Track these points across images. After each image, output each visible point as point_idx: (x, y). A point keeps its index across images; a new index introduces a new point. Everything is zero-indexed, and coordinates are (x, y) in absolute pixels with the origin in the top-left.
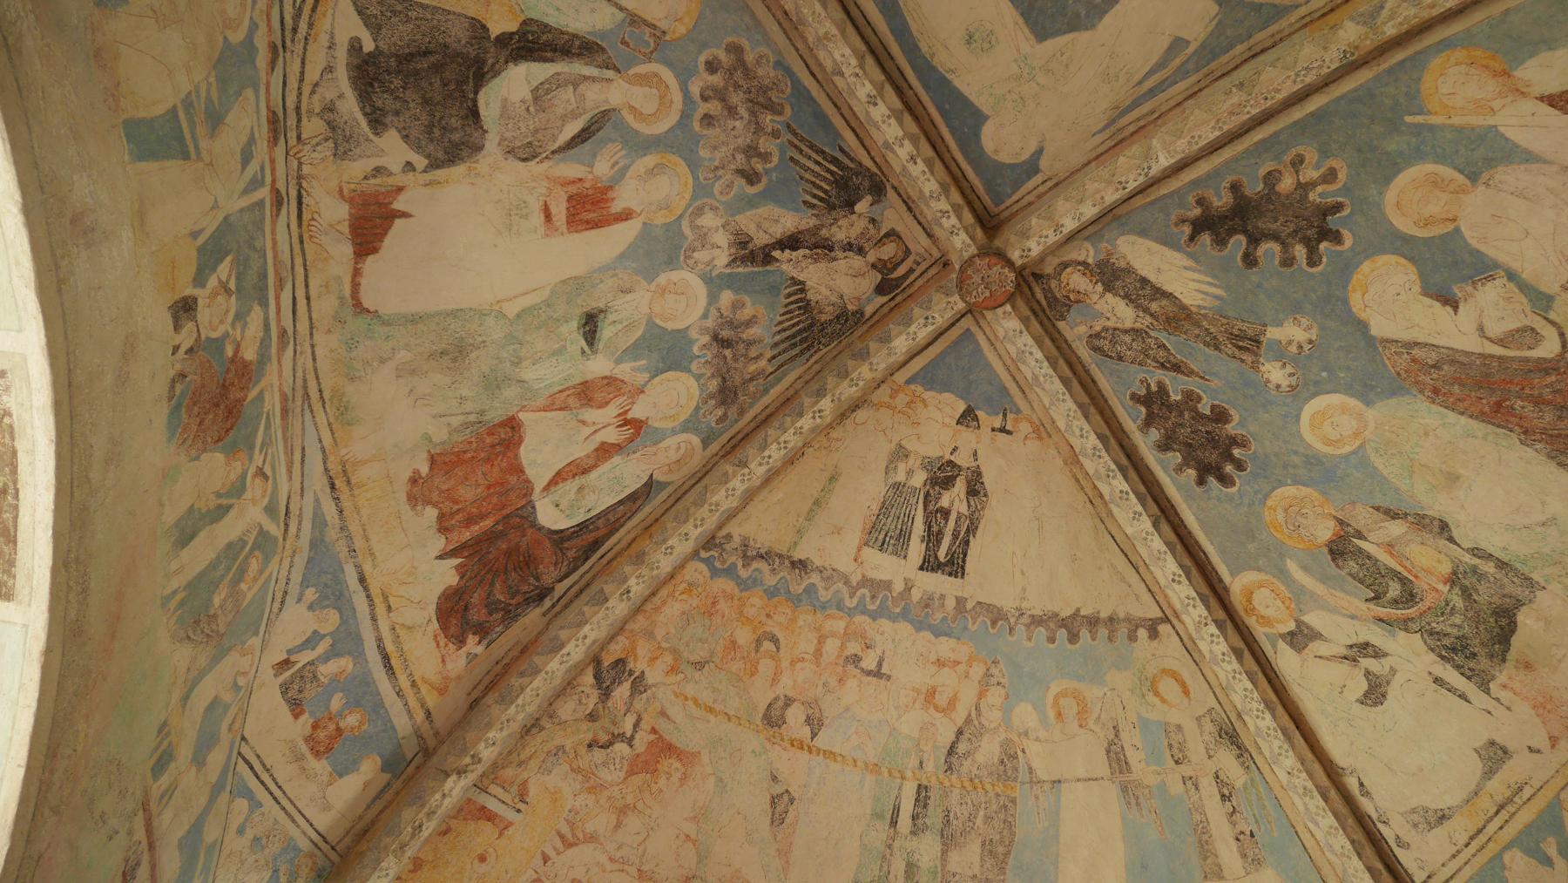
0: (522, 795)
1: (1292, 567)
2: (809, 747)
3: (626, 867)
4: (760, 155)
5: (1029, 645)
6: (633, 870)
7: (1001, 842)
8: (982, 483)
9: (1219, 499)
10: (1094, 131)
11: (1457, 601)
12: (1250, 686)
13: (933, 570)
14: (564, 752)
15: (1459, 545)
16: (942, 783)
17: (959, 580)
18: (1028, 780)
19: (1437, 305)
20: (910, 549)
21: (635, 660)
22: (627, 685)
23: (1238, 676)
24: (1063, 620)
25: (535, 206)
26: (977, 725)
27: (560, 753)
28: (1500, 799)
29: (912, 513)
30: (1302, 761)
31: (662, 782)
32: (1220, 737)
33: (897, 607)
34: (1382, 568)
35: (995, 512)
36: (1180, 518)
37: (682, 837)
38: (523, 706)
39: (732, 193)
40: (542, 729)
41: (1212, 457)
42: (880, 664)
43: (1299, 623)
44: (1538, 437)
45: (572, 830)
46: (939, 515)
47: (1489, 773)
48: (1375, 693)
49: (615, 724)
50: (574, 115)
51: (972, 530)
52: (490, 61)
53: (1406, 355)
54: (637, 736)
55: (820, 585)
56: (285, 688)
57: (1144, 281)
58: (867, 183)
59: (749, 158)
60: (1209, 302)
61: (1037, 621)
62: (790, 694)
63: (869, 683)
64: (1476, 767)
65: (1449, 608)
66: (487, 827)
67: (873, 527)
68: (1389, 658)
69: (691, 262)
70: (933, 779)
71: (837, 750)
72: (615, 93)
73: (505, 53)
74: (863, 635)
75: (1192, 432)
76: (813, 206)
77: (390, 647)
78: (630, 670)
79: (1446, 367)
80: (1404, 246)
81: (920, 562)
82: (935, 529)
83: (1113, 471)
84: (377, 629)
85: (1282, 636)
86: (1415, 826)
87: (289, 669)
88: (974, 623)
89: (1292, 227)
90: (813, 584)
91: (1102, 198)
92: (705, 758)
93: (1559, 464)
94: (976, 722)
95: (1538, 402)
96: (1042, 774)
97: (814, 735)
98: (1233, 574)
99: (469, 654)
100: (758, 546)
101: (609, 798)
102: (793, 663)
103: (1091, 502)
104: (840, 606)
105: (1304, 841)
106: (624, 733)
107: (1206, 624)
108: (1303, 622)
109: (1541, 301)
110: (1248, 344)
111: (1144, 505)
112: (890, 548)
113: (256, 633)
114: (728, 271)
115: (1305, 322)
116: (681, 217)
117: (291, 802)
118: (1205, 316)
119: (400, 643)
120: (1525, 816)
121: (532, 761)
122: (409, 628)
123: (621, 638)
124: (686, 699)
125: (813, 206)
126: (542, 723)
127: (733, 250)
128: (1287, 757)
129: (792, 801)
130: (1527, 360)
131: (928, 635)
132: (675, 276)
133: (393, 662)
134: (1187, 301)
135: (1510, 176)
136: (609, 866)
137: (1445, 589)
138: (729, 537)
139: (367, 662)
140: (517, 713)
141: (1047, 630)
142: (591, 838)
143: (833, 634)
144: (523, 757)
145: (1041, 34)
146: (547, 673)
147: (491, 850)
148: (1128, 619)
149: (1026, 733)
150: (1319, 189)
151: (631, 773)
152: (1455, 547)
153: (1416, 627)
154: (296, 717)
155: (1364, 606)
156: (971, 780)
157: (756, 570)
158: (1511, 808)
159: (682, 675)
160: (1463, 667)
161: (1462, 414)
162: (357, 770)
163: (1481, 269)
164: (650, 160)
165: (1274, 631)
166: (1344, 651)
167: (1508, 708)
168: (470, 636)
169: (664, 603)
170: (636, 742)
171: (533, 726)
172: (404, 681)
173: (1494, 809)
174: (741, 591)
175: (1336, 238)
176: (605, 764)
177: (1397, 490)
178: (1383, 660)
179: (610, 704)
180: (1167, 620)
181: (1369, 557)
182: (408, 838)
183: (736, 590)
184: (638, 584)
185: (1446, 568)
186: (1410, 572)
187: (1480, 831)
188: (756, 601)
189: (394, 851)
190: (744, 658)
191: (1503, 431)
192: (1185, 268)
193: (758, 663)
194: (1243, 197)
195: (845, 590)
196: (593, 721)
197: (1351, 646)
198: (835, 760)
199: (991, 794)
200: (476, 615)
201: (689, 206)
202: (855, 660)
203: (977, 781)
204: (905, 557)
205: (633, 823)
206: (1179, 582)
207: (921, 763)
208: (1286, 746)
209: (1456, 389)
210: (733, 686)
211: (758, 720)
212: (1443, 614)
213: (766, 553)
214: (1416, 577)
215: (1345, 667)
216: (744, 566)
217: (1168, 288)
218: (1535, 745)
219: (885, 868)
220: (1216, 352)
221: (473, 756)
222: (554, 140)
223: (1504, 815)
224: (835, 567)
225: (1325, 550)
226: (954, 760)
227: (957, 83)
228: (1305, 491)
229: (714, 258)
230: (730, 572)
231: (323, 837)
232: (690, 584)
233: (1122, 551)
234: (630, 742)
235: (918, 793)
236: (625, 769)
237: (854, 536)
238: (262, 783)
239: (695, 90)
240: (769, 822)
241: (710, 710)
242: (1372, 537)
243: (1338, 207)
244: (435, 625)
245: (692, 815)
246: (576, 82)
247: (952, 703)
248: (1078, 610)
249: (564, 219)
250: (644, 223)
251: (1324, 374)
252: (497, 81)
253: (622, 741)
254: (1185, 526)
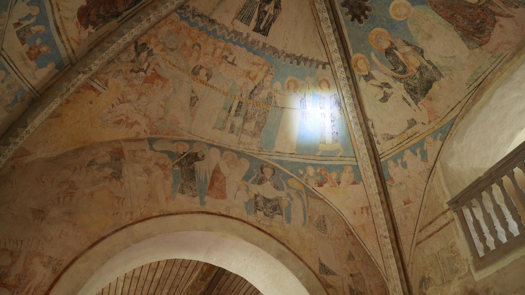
0: (106, 84)
1: (373, 54)
2: (206, 83)
3: (140, 112)
5: (284, 63)
6: (142, 114)
7: (262, 123)
8: (280, 5)
9: (356, 27)
11: (418, 76)
12: (349, 89)
13: (258, 32)
14: (122, 72)
15: (424, 58)
16: (247, 102)
17: (265, 37)
18: (274, 105)
20: (251, 23)
21: (150, 44)
22: (146, 53)
23: (346, 85)
24: (296, 57)
26: (262, 86)
27: (120, 72)
28: (409, 135)
29: (254, 10)
30: (358, 114)
31: (155, 87)
32: (336, 103)
33: (243, 42)
34: (399, 61)
35: (283, 16)
36: (342, 31)
37: (160, 105)
38: (108, 53)
40: (114, 63)
41: (358, 12)
42: (234, 60)
43: (369, 73)
44: (460, 29)
45: (123, 98)
46: (263, 13)
47: (409, 128)
48: (385, 99)
49: (140, 65)
51: (273, 20)
54: (148, 70)
55: (218, 30)
56: (18, 33)
61: (288, 56)
62: (202, 65)
63: (229, 66)
64: (406, 125)
65: (415, 77)
66: (93, 93)
67: (240, 13)
68: (392, 89)
70: (244, 100)
71: (215, 86)
74: (229, 50)
75: (354, 2)
77: (59, 25)
78: (148, 48)
81: (254, 28)
82: (261, 17)
83: (325, 10)
84: (54, 17)
85: (363, 76)
86: (384, 138)
87: (20, 26)
88: (267, 53)
90: (216, 29)
92: (170, 81)
93: (463, 39)
94: (261, 85)
95: (464, 17)
96: (279, 105)
97: (208, 80)
98: (353, 53)
99: (89, 32)
100: (198, 11)
101: (136, 90)
102: (205, 55)
103: (315, 19)
104: (224, 38)
105: (351, 138)
106: (143, 69)
107: (341, 67)
108: (370, 73)
111: (332, 24)
112: (244, 21)
113: (6, 11)
117: (22, 74)
119: (63, 24)
120: (414, 141)
121: (110, 73)
122: (67, 19)
123: (145, 36)
124: (166, 61)
126: (115, 61)
128: (354, 113)
129: (198, 100)
131: (251, 53)
133: (60, 30)
136: (134, 111)
137: (415, 71)
138: (188, 6)
139: (50, 28)
140: (106, 56)
141: (291, 59)
142: (129, 101)
143: (220, 48)
144: (107, 71)
146: (118, 43)
147: (94, 100)
148: (317, 61)
149: (277, 91)
151: (145, 82)
152: (423, 59)
153: (403, 81)
154: (23, 44)
155: (390, 71)
156: (256, 102)
157: (196, 20)
158: (411, 139)
159: (166, 53)
160: (412, 96)
161: (440, 16)
162: (46, 67)
165: (361, 74)
166: (380, 84)
167: (421, 111)
168: (90, 26)
169: (162, 26)
170: (147, 72)
171: (111, 61)
172: (64, 37)
173: (407, 138)
174: (190, 27)
176: (136, 78)
177: (412, 36)
178: (390, 89)
179: (139, 58)
180: (329, 64)
181: (397, 56)
182: (65, 92)
183: (189, 26)
184: (153, 17)
185: (418, 65)
186: (407, 64)
187: (401, 143)
188: (195, 31)
189: (59, 96)
190: (188, 50)
193: (193, 52)
195: (226, 33)
196: (133, 63)
197: (382, 83)
198: (214, 89)
199: (262, 108)
200: (93, 18)
202: (226, 57)
203: (258, 103)
204: (249, 25)
205: (144, 98)
206: (336, 52)
207: (241, 95)
208: (354, 109)
209: (442, 7)
210: (183, 59)
211: (190, 72)
212: (412, 79)
213: (201, 15)
214: (408, 66)
215: (379, 89)
216: (192, 18)
218: (424, 122)
219: (224, 125)
221: (89, 68)
223: (409, 140)
224: (224, 24)
225: (384, 51)
226: (252, 95)
228: (384, 30)
230: (187, 19)
231: (34, 88)
232: (172, 21)
233: (321, 38)
234: (145, 72)
235: (239, 104)
236: (143, 81)
237: (232, 15)
238: (10, 66)
240: (189, 105)
241: (174, 66)
242: (399, 50)
244: (77, 19)
245: (164, 99)
247: (255, 77)
248: (302, 55)
253: (143, 71)
254: (343, 34)
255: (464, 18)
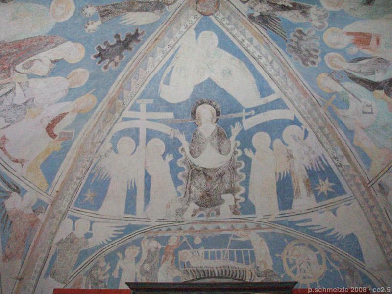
4: (297, 37)
10: (180, 48)
19: (57, 58)
25: (382, 45)
39: (309, 29)
50: (362, 65)
52: (386, 84)
53: (56, 41)
57: (147, 10)
58: (256, 20)
59: (301, 37)
60: (123, 17)
69: (325, 12)
72: (346, 66)
73: (380, 85)
76: (276, 18)
79: (42, 46)
80: (77, 66)
89: (110, 51)
91: (175, 40)
95: (10, 54)
109: (31, 76)
110: (104, 13)
114: (311, 5)
115: (92, 32)
116: (328, 28)
118: (122, 12)
125: (276, 18)
127: (308, 11)
130: (22, 62)
132: (332, 9)
134: (131, 13)
135: (61, 94)
145: (209, 80)
150: (107, 63)
161: (28, 38)
163: (52, 73)
164: (339, 47)
175: (96, 57)
191: (12, 41)
192: (135, 22)
194: (127, 49)
201: (326, 29)
209: (35, 44)
217: (138, 13)
220: (113, 4)
222: (370, 62)
227: (230, 56)
229: (316, 11)
239: (319, 59)
243: (100, 62)
246: (360, 72)
249: (372, 39)
250: (342, 29)
251: (76, 22)
252: (385, 79)
255: (10, 54)
